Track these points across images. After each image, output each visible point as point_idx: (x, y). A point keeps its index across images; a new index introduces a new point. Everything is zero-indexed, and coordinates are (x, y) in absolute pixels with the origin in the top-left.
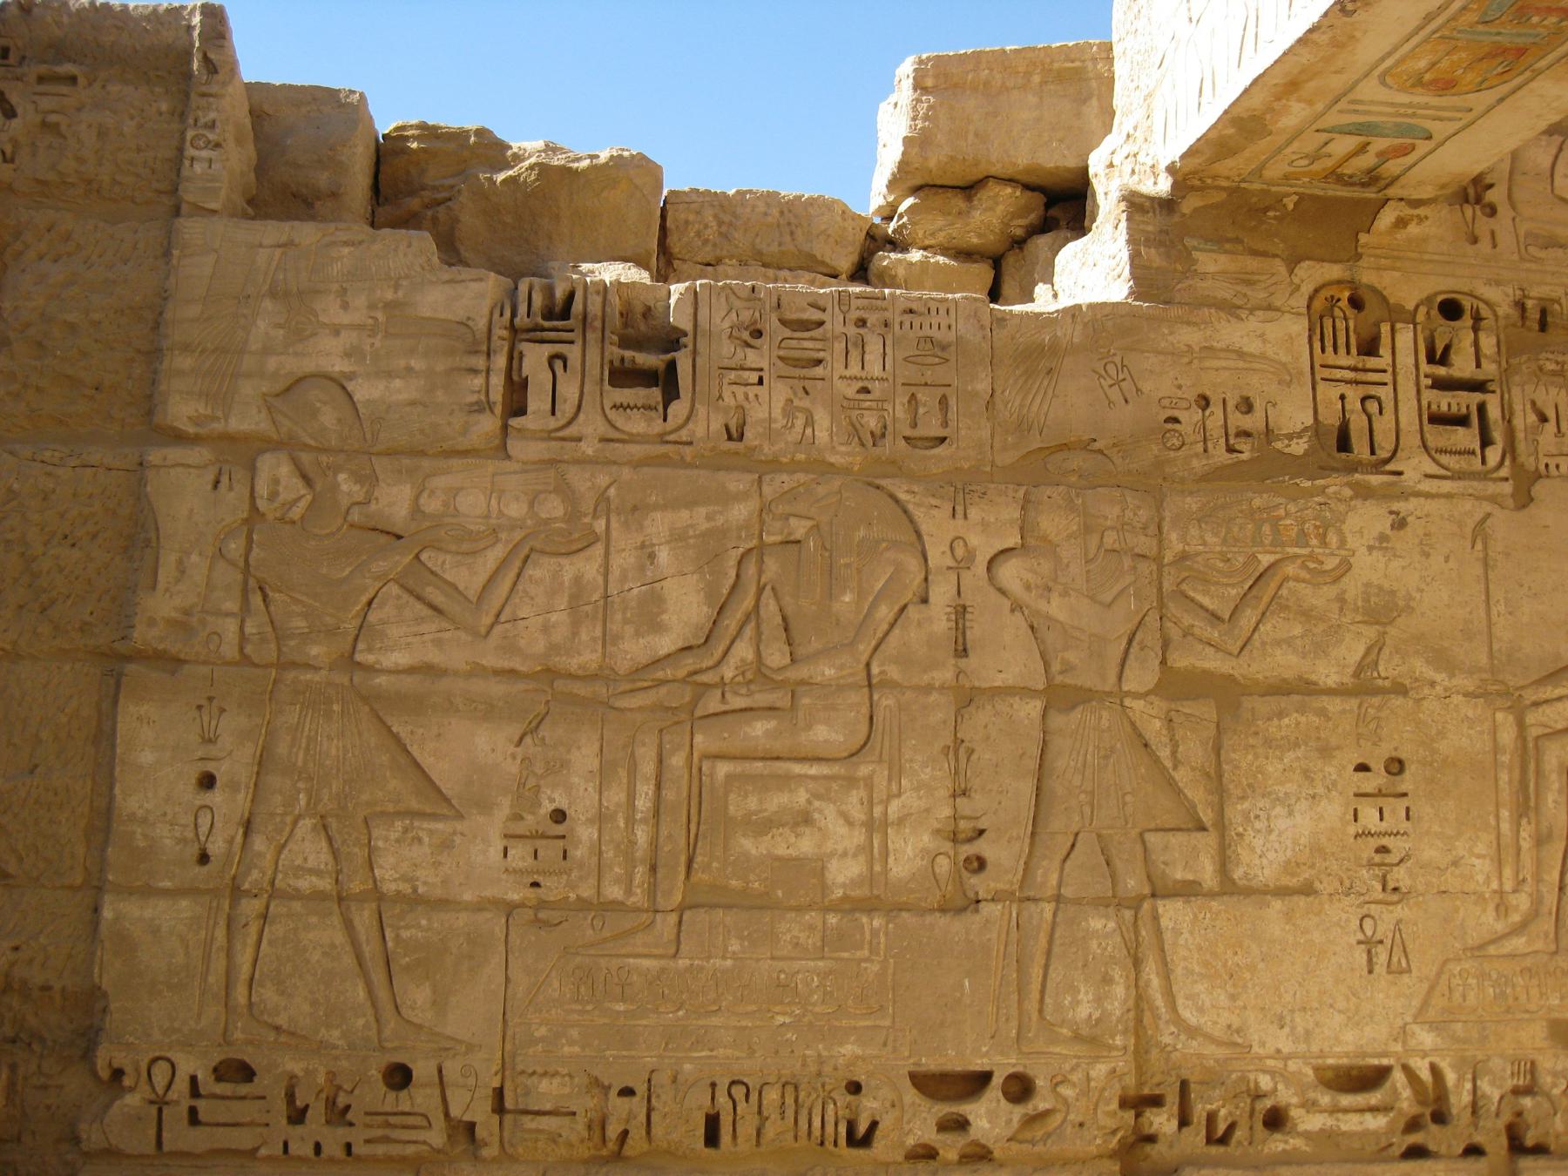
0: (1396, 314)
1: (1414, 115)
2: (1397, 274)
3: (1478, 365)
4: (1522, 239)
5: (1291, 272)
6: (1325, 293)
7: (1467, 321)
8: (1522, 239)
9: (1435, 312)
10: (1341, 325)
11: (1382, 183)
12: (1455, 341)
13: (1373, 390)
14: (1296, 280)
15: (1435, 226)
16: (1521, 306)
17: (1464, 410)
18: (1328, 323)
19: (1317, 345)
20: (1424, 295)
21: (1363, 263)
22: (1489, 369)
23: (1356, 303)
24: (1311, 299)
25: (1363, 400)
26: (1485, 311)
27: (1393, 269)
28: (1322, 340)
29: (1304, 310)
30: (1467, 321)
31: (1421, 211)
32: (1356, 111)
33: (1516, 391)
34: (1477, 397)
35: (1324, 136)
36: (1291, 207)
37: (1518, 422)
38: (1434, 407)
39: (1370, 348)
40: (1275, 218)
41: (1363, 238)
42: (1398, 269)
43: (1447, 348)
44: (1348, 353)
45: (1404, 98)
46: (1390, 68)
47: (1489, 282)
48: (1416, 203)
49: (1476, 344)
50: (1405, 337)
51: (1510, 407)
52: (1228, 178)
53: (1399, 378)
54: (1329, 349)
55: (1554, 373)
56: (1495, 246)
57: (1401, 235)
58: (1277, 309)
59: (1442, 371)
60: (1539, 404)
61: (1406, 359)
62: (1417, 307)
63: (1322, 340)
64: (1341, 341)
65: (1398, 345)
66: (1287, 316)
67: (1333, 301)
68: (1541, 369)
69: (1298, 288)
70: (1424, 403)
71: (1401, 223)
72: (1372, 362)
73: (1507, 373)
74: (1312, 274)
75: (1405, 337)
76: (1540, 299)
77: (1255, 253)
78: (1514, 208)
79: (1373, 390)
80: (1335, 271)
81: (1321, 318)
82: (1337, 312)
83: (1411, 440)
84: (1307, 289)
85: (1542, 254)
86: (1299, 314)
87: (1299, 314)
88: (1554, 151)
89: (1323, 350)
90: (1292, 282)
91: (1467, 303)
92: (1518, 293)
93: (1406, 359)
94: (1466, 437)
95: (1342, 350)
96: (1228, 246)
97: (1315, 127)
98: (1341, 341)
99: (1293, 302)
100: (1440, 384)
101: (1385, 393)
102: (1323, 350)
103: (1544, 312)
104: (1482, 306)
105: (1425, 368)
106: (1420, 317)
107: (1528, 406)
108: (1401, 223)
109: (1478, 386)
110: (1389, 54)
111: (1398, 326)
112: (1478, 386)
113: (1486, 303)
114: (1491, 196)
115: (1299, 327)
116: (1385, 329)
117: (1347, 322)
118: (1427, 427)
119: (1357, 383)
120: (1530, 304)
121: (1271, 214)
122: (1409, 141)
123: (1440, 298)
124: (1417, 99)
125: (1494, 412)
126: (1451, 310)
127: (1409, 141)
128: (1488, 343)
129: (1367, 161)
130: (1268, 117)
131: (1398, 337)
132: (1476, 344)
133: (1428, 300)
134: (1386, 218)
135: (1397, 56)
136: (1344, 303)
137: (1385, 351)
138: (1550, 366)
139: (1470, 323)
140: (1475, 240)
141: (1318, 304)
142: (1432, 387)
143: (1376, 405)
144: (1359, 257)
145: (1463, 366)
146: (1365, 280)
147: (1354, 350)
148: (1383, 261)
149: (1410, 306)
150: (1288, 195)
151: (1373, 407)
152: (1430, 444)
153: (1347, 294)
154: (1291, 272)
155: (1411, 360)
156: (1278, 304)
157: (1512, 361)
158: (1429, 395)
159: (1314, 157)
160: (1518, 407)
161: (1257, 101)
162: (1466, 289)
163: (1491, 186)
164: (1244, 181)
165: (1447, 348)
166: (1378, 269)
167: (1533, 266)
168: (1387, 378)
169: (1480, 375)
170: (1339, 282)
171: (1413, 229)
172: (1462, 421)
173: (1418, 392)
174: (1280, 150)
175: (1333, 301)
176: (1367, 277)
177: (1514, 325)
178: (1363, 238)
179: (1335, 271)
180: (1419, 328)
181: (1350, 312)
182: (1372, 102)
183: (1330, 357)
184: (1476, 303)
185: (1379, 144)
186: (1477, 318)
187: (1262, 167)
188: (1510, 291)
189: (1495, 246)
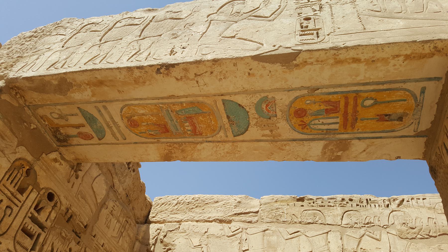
0: (36, 186)
1: (110, 128)
2: (45, 174)
3: (46, 221)
4: (79, 191)
5: (17, 146)
6: (21, 162)
7: (52, 204)
8: (79, 191)
9: (46, 194)
10: (19, 176)
11: (65, 144)
12: (46, 207)
13: (13, 206)
14: (17, 150)
15: (63, 169)
16: (68, 210)
17: (34, 232)
18: (16, 172)
19: (7, 176)
20: (47, 186)
21: (39, 163)
22: (48, 224)
23: (28, 172)
24: (16, 160)
25: (7, 207)
26: (58, 205)
27: (45, 172)
28: (10, 176)
29: (12, 162)
30: (52, 204)
31: (62, 162)
32: (100, 111)
33: (51, 236)
34: (40, 231)
35: (78, 111)
36: (32, 128)
37: (45, 247)
38: (26, 225)
39: (21, 191)
40: (25, 126)
41: (44, 155)
42: (46, 173)
43: (42, 208)
44: (14, 187)
45: (117, 119)
46: (132, 105)
47: (65, 197)
48: (63, 158)
49: (50, 213)
50: (33, 196)
51: (46, 241)
52: (25, 101)
53: (23, 207)
54: (10, 181)
55: (63, 237)
56: (72, 187)
57: (53, 164)
58: (4, 154)
59: (36, 214)
60: (54, 245)
61: (29, 203)
62: (43, 188)
63: (10, 176)
64: (15, 181)
65: (30, 196)
66: (5, 159)
67: (22, 166)
68: (61, 234)
69: (15, 153)
70: (25, 222)
71: (55, 160)
72: (19, 196)
73: (52, 228)
74: (23, 153)
75: (33, 196)
76: (73, 212)
77: (11, 130)
78: (82, 181)
79: (13, 206)
80: (29, 158)
81: (15, 169)
82: (21, 171)
83: (12, 233)
84: (18, 156)
85: (80, 199)
86: (9, 161)
87: (9, 161)
88: (98, 174)
89: (7, 180)
90: (15, 150)
91: (56, 198)
92: (69, 206)
93: (29, 203)
94: (28, 243)
95: (13, 184)
96: (6, 120)
97: (80, 106)
98: (15, 181)
99: (11, 156)
100: (34, 220)
101: (16, 209)
102: (7, 180)
103: (71, 216)
104: (59, 202)
105: (32, 210)
106: (41, 193)
107: (51, 244)
108: (55, 160)
109: (42, 227)
110: (141, 99)
111: (34, 190)
112: (42, 227)
113: (60, 202)
114: (79, 173)
115: (6, 165)
116: (30, 188)
117: (20, 176)
118: (20, 231)
119: (10, 199)
120: (70, 211)
121: (25, 124)
122: (94, 135)
123: (50, 191)
124: (121, 124)
125: (41, 240)
126: (51, 197)
127: (94, 135)
128: (53, 215)
129: (73, 132)
130: (74, 88)
131: (32, 194)
132: (50, 213)
133: (47, 189)
134: (53, 155)
135: (141, 102)
136: (25, 170)
137: (25, 195)
138: (63, 235)
139: (53, 205)
140: (69, 182)
141: (17, 163)
142: (30, 218)
143: (10, 211)
144: (38, 159)
145: (42, 217)
146: (35, 168)
147: (17, 188)
148: (44, 167)
149: (42, 187)
150: (34, 124)
151: (9, 211)
152: (17, 238)
153: (28, 168)
154: (17, 146)
155: (30, 204)
156: (6, 152)
157: (55, 225)
158: (28, 220)
159: (61, 117)
160: (48, 242)
161: (80, 78)
162: (58, 194)
163: (81, 170)
164: (28, 107)
165: (42, 208)
166: (41, 168)
167: (77, 201)
168: (20, 204)
169: (45, 224)
170: (28, 162)
171: (57, 165)
172: (31, 236)
173: (25, 217)
174: (56, 104)
175: (22, 166)
176: (36, 168)
177: (62, 215)
178: (44, 155)
179: (29, 158)
180: (39, 195)
181: (24, 174)
182: (109, 113)
183: (8, 184)
184: (58, 200)
185: (87, 129)
186: (55, 205)
187: (42, 106)
188: (68, 203)
189: (72, 187)
